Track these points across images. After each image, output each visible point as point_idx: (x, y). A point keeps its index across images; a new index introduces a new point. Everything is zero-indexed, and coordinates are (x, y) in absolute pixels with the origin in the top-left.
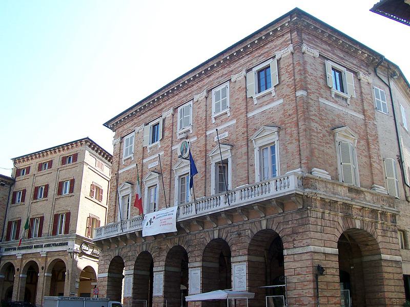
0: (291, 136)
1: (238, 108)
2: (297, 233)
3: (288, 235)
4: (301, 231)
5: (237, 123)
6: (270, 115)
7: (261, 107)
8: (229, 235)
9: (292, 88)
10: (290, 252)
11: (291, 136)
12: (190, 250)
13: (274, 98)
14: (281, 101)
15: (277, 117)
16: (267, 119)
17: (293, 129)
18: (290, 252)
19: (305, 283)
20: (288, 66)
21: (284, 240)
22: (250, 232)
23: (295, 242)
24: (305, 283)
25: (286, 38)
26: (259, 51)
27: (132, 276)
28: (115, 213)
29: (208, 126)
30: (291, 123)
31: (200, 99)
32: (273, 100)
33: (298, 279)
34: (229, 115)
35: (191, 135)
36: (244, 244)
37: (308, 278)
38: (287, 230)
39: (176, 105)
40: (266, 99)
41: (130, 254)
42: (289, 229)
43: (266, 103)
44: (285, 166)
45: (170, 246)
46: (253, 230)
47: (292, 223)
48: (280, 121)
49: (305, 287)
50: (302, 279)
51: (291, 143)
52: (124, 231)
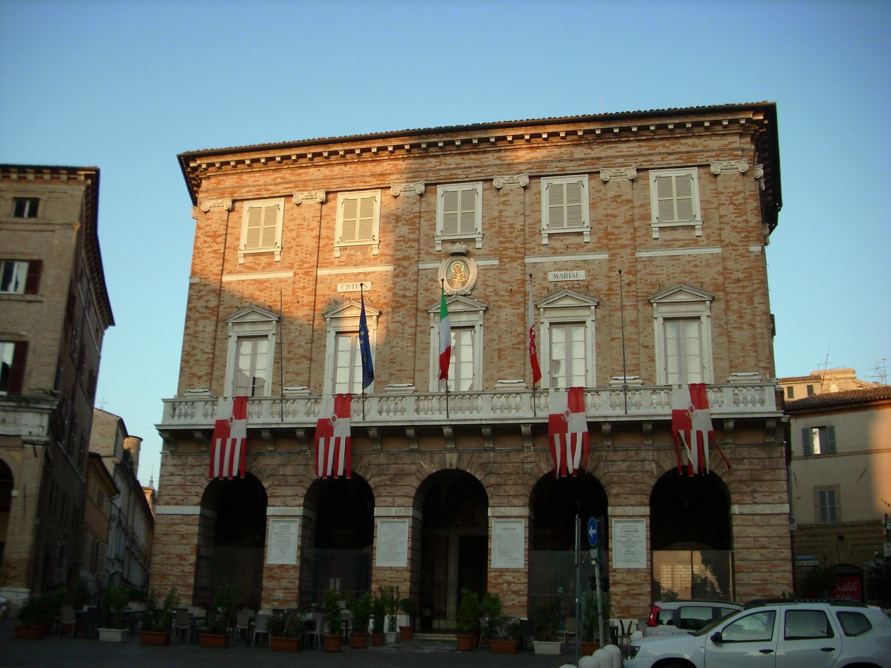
0: (741, 317)
1: (613, 234)
2: (760, 481)
3: (741, 482)
4: (767, 477)
5: (610, 261)
6: (689, 268)
7: (669, 246)
8: (602, 464)
9: (743, 235)
10: (746, 509)
11: (741, 317)
12: (492, 480)
13: (701, 239)
14: (718, 250)
15: (709, 275)
16: (683, 272)
17: (744, 306)
18: (746, 509)
19: (776, 563)
20: (734, 194)
21: (731, 488)
22: (654, 465)
23: (757, 495)
24: (776, 563)
25: (730, 143)
26: (667, 143)
27: (299, 521)
28: (212, 366)
29: (527, 246)
30: (739, 294)
31: (507, 188)
32: (695, 242)
33: (762, 555)
34: (587, 239)
35: (478, 252)
36: (639, 486)
37: (782, 555)
38: (739, 473)
39: (432, 177)
40: (679, 234)
41: (288, 470)
42: (745, 473)
43: (681, 243)
44: (725, 364)
45: (429, 468)
46: (662, 463)
47: (751, 463)
48: (712, 284)
49: (776, 569)
50: (770, 555)
51: (740, 328)
52: (286, 420)
